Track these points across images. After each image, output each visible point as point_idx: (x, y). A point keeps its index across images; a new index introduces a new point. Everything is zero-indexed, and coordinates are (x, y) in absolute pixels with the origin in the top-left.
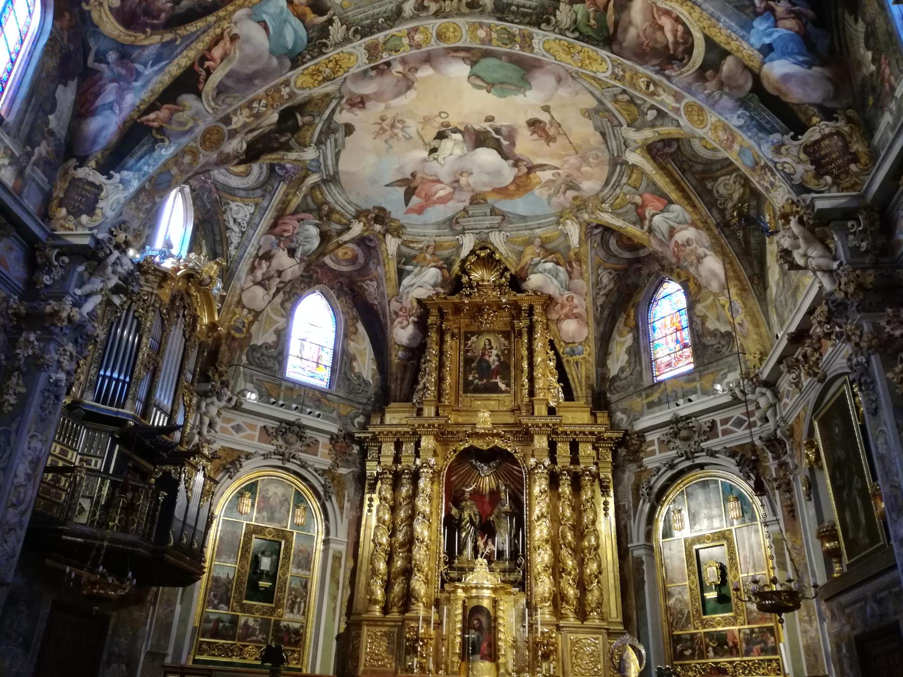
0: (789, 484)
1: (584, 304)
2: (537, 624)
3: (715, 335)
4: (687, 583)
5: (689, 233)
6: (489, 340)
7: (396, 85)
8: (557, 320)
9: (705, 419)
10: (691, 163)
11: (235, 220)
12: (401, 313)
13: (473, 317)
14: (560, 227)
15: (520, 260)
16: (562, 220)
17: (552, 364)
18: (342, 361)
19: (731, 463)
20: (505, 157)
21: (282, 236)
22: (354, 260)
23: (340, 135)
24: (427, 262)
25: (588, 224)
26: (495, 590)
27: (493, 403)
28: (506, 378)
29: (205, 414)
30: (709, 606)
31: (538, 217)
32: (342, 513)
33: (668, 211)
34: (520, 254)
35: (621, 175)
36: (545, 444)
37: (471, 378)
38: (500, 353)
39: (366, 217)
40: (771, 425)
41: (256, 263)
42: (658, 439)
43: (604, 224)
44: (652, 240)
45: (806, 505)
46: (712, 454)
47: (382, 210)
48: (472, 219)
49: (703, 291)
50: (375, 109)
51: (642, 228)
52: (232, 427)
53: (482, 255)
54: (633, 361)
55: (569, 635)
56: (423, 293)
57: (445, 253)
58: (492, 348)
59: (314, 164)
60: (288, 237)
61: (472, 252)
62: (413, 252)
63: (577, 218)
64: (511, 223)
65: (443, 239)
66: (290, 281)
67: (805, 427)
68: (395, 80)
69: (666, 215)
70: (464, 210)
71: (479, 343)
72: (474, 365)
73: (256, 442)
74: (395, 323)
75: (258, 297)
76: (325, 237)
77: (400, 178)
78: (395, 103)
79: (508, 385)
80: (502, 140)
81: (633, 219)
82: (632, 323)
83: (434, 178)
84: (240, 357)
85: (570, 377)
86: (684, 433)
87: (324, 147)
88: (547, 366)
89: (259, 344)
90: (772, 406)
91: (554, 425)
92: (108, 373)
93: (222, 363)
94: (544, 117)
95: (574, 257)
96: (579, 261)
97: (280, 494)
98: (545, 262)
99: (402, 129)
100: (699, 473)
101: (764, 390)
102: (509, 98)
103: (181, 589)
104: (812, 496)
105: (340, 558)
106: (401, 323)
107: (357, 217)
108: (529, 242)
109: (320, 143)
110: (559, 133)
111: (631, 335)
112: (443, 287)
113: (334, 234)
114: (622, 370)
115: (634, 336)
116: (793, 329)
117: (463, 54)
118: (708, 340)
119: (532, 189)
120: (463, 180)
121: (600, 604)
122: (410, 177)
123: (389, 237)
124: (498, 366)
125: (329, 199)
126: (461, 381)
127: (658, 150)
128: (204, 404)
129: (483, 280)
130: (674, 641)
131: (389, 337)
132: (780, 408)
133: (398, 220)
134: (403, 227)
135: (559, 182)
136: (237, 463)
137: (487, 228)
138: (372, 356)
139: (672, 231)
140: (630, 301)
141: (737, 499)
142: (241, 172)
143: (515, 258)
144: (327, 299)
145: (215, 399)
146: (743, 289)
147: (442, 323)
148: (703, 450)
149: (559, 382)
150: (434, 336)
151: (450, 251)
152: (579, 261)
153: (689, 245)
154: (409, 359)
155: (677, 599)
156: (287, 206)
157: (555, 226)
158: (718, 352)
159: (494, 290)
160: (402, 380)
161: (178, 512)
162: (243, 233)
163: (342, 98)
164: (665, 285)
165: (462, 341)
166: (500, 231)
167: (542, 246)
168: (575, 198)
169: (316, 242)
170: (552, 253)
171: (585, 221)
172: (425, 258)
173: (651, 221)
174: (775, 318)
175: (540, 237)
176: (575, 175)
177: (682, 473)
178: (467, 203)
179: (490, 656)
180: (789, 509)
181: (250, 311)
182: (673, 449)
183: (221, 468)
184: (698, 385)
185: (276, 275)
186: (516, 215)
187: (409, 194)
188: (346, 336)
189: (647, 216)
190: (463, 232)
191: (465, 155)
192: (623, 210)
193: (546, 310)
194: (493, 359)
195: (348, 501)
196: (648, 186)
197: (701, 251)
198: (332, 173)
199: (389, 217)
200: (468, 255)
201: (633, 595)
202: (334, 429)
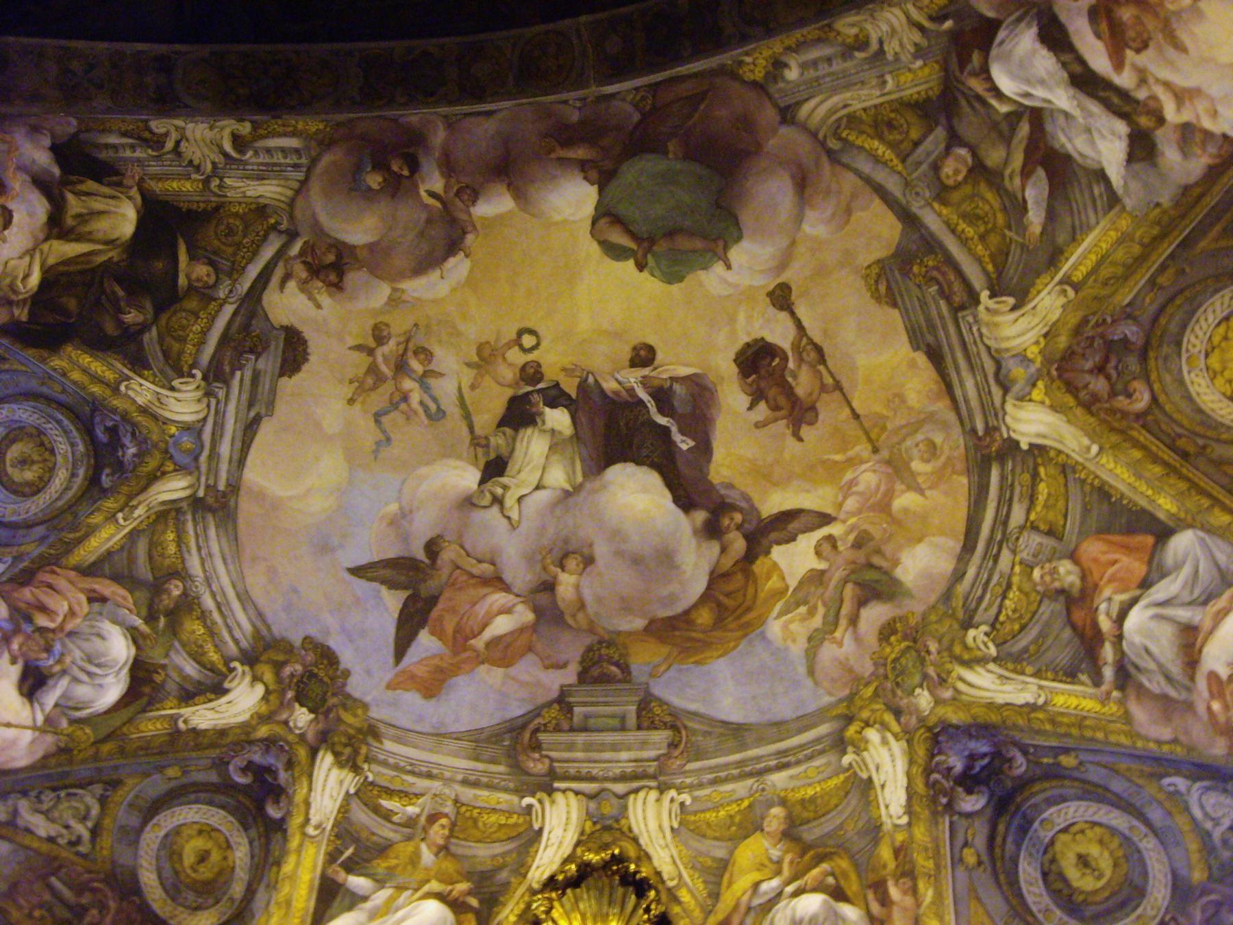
7: (421, 234)
10: (1200, 442)
14: (847, 759)
15: (715, 896)
16: (851, 731)
20: (685, 500)
21: (29, 619)
23: (268, 363)
24: (419, 876)
31: (780, 728)
33: (1163, 576)
35: (1006, 502)
39: (278, 666)
47: (328, 657)
48: (580, 738)
50: (370, 296)
51: (1097, 680)
57: (483, 853)
59: (187, 442)
60: (42, 630)
62: (386, 832)
63: (897, 713)
64: (700, 755)
68: (424, 216)
69: (1161, 591)
70: (563, 701)
76: (143, 682)
77: (391, 554)
78: (415, 287)
80: (677, 437)
81: (1063, 656)
83: (486, 568)
87: (221, 394)
94: (780, 333)
95: (892, 865)
96: (908, 873)
98: (797, 894)
99: (422, 380)
102: (690, 280)
107: (250, 659)
108: (750, 825)
109: (216, 375)
110: (823, 388)
113: (171, 686)
117: (581, 153)
119: (762, 620)
120: (567, 583)
122: (421, 555)
123: (326, 760)
125: (194, 564)
127: (1095, 398)
133: (366, 706)
134: (372, 731)
135: (838, 575)
137: (623, 778)
139: (1191, 642)
142: (29, 484)
151: (498, 849)
152: (908, 873)
156: (80, 541)
163: (292, 235)
166: (662, 789)
167: (790, 834)
168: (887, 632)
169: (112, 690)
170: (820, 859)
171: (922, 720)
172: (415, 859)
173: (1120, 637)
175: (783, 802)
176: (876, 532)
178: (569, 676)
186: (712, 721)
187: (412, 621)
189: (1105, 624)
190: (546, 785)
191: (578, 489)
192: (1033, 632)
196: (1086, 510)
198: (222, 486)
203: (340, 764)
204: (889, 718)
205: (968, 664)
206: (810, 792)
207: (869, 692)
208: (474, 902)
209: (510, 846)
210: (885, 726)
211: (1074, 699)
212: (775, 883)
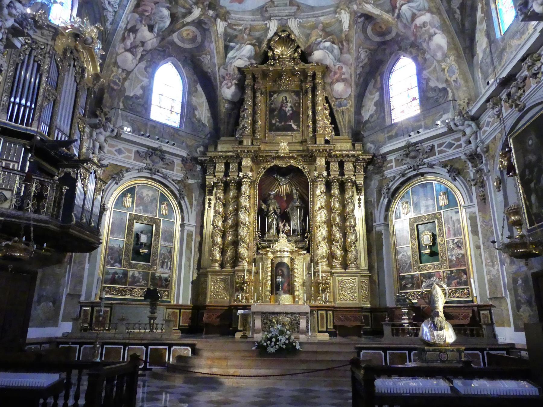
0: (482, 182)
1: (349, 71)
2: (319, 272)
3: (435, 91)
4: (410, 245)
5: (426, 17)
6: (286, 97)
8: (331, 83)
9: (427, 145)
11: (109, 3)
12: (227, 77)
13: (275, 81)
14: (337, 16)
15: (308, 40)
16: (338, 10)
17: (327, 112)
18: (188, 110)
19: (444, 171)
21: (144, 15)
22: (193, 40)
25: (355, 13)
26: (292, 252)
27: (288, 137)
29: (96, 140)
30: (424, 258)
31: (322, 8)
32: (191, 208)
34: (308, 36)
36: (324, 163)
37: (274, 122)
38: (293, 105)
39: (203, 3)
40: (473, 146)
41: (126, 35)
42: (395, 158)
43: (367, 13)
44: (399, 24)
45: (495, 193)
46: (431, 166)
48: (276, 8)
49: (427, 62)
51: (393, 15)
52: (116, 151)
53: (283, 36)
54: (379, 110)
55: (337, 278)
56: (241, 63)
57: (257, 34)
58: (287, 102)
60: (147, 16)
61: (276, 34)
62: (235, 33)
63: (349, 8)
65: (256, 23)
66: (150, 50)
67: (500, 144)
69: (412, 4)
71: (279, 98)
72: (275, 113)
73: (132, 161)
74: (223, 84)
75: (128, 60)
76: (174, 17)
79: (298, 126)
82: (379, 86)
84: (118, 103)
85: (338, 121)
86: (412, 154)
88: (324, 114)
89: (131, 95)
90: (475, 133)
91: (330, 150)
92: (18, 100)
93: (106, 106)
96: (348, 41)
97: (150, 195)
98: (325, 42)
100: (420, 178)
101: (470, 122)
103: (88, 254)
104: (501, 188)
105: (192, 235)
106: (227, 84)
111: (378, 93)
112: (255, 59)
113: (180, 15)
114: (371, 116)
115: (380, 94)
116: (504, 75)
118: (431, 94)
121: (356, 259)
123: (219, 20)
124: (291, 114)
126: (268, 124)
128: (94, 134)
129: (282, 55)
130: (400, 279)
131: (218, 93)
132: (480, 133)
133: (226, 8)
134: (228, 12)
136: (120, 174)
137: (286, 16)
138: (208, 108)
139: (414, 17)
141: (445, 194)
143: (305, 39)
144: (176, 68)
145: (102, 130)
146: (458, 57)
147: (254, 85)
148: (425, 164)
149: (331, 124)
150: (249, 92)
151: (260, 33)
153: (425, 27)
154: (232, 109)
155: (403, 255)
157: (333, 15)
158: (436, 101)
159: (290, 61)
161: (78, 201)
162: (116, 12)
164: (401, 60)
165: (268, 98)
166: (295, 18)
167: (323, 30)
169: (168, 22)
172: (243, 38)
173: (400, 9)
174: (480, 75)
177: (409, 179)
179: (289, 291)
180: (482, 198)
181: (123, 70)
182: (405, 164)
183: (110, 177)
184: (423, 124)
185: (140, 45)
188: (190, 93)
189: (398, 5)
190: (270, 19)
193: (323, 77)
194: (288, 109)
195: (195, 200)
197: (432, 31)
199: (219, 5)
200: (273, 36)
201: (375, 254)
202: (184, 154)
203: (222, 20)
204: (347, 9)
205: (367, 3)
206: (328, 21)
207: (343, 3)
208: (257, 44)
209: (262, 32)
210: (345, 10)
211: (387, 17)
212: (320, 39)
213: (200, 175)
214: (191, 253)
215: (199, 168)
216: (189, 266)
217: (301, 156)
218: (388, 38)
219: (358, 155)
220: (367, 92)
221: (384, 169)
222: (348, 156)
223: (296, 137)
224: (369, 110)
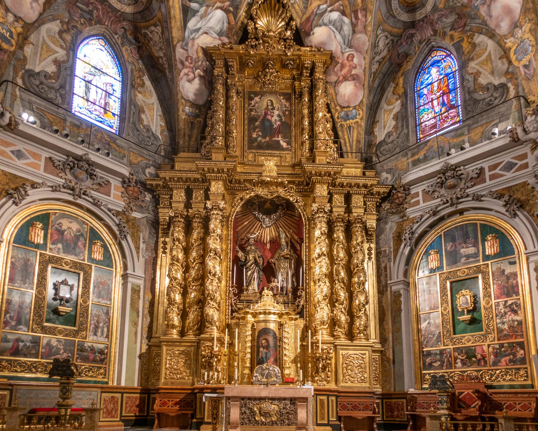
12: (187, 63)
13: (257, 77)
18: (130, 110)
28: (287, 137)
71: (262, 103)
74: (182, 74)
105: (139, 291)
106: (187, 74)
140: (399, 70)
143: (302, 6)
147: (227, 78)
160: (190, 137)
165: (246, 100)
213: (151, 208)
214: (138, 316)
215: (148, 197)
216: (136, 334)
217: (293, 182)
218: (419, 15)
219: (372, 185)
220: (383, 101)
221: (405, 206)
222: (358, 186)
223: (286, 158)
224: (387, 124)
